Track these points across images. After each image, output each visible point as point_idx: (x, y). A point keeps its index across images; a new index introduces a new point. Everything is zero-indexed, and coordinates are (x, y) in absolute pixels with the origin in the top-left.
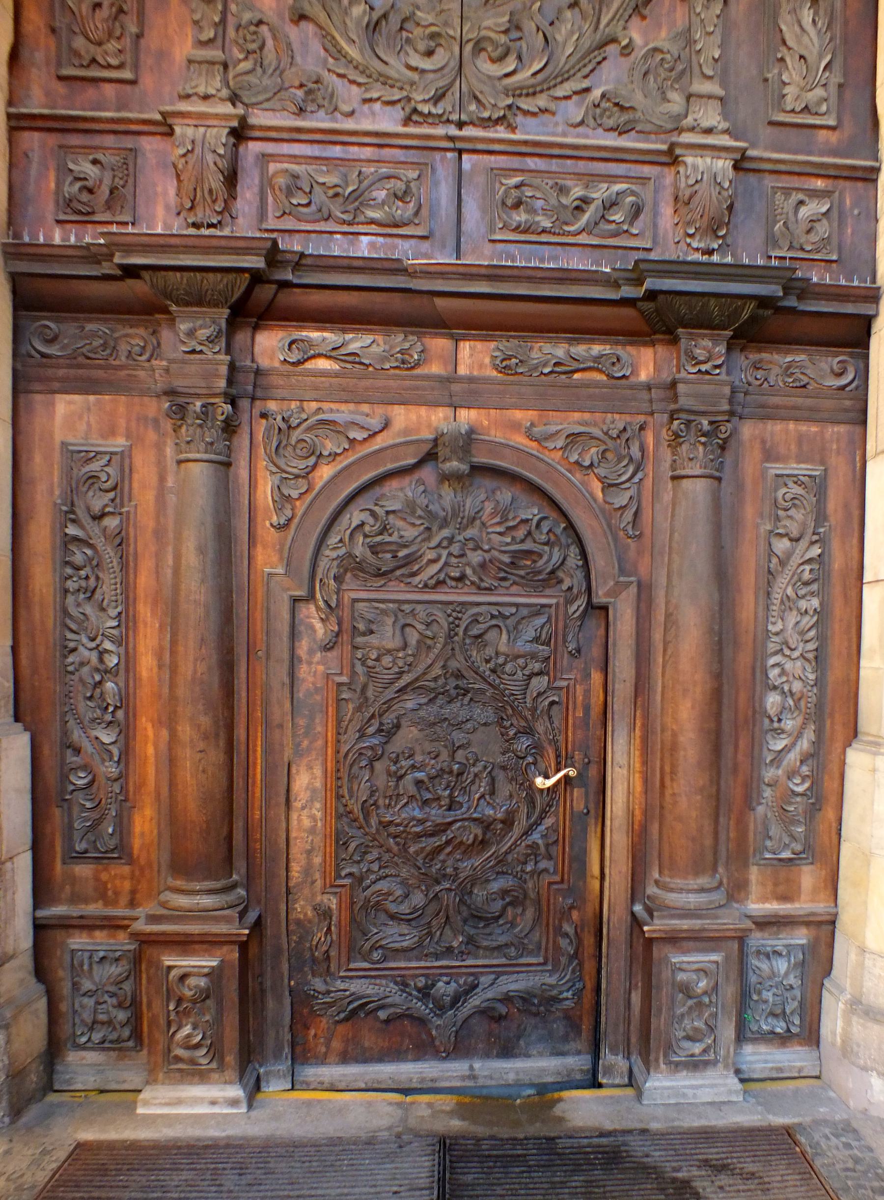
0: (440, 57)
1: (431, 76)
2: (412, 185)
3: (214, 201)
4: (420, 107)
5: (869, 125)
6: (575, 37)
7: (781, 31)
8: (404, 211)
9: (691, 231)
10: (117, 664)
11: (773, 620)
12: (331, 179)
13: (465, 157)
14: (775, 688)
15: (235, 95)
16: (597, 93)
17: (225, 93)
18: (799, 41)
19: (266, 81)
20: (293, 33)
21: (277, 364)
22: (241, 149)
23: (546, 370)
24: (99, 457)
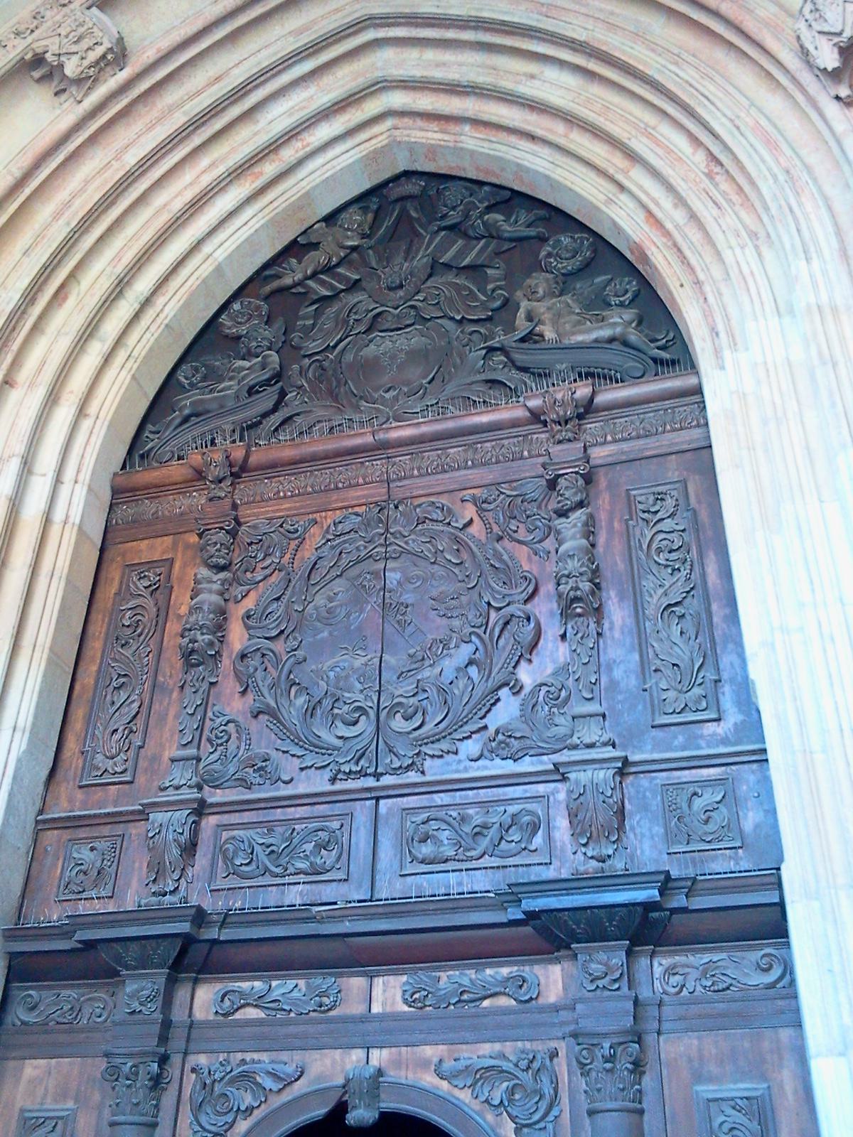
16: (492, 729)
20: (254, 726)
21: (211, 1017)
22: (203, 823)
24: (47, 1122)
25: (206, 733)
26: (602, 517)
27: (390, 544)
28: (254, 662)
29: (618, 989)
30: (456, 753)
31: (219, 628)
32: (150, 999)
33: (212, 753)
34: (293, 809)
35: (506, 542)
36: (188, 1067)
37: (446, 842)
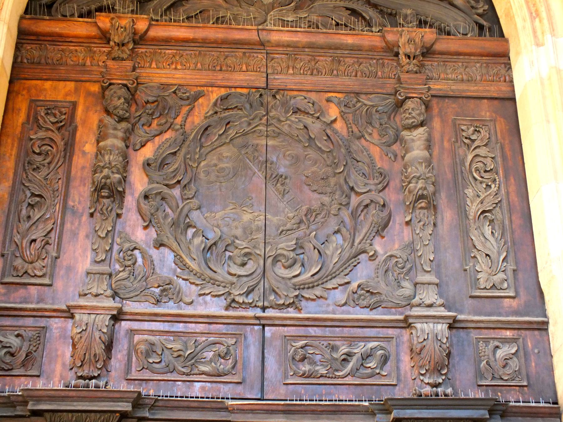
0: (251, 266)
1: (245, 279)
2: (231, 348)
3: (97, 362)
4: (237, 299)
5: (537, 293)
6: (339, 252)
7: (472, 240)
8: (225, 365)
12: (177, 346)
13: (267, 328)
15: (115, 292)
16: (354, 285)
17: (109, 292)
18: (484, 246)
19: (136, 284)
20: (154, 253)
26: (437, 135)
27: (270, 125)
34: (193, 325)
37: (319, 363)
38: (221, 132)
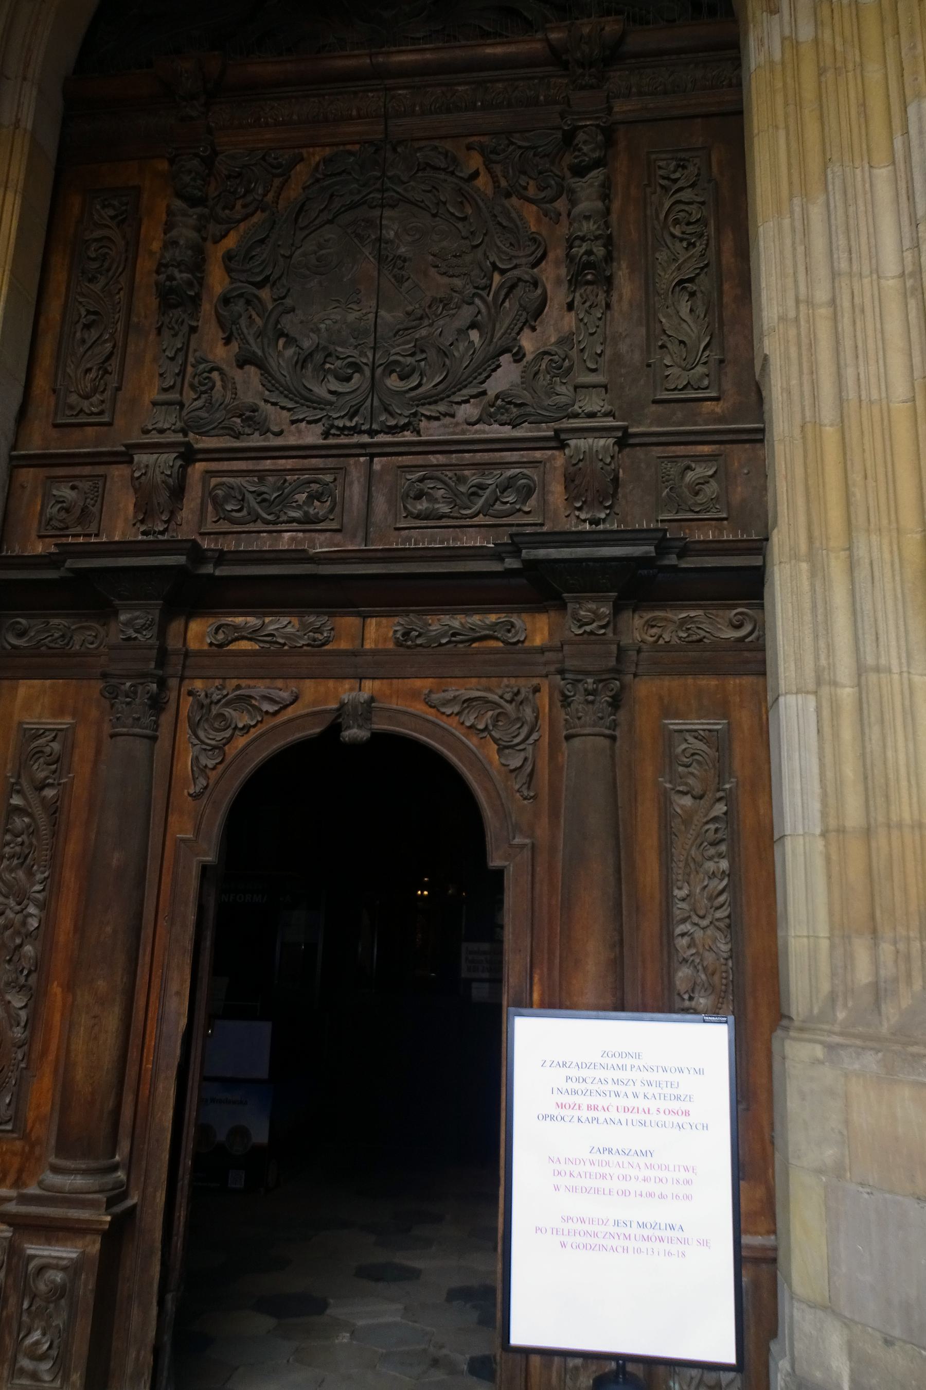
3: (162, 513)
4: (336, 423)
9: (578, 505)
10: (37, 928)
11: (679, 884)
13: (376, 460)
14: (685, 960)
20: (238, 375)
21: (206, 647)
22: (190, 470)
23: (444, 641)
24: (47, 733)
25: (188, 378)
27: (387, 190)
28: (239, 306)
29: (604, 634)
30: (453, 416)
31: (198, 265)
32: (144, 627)
33: (195, 400)
35: (514, 200)
36: (184, 690)
38: (322, 207)
